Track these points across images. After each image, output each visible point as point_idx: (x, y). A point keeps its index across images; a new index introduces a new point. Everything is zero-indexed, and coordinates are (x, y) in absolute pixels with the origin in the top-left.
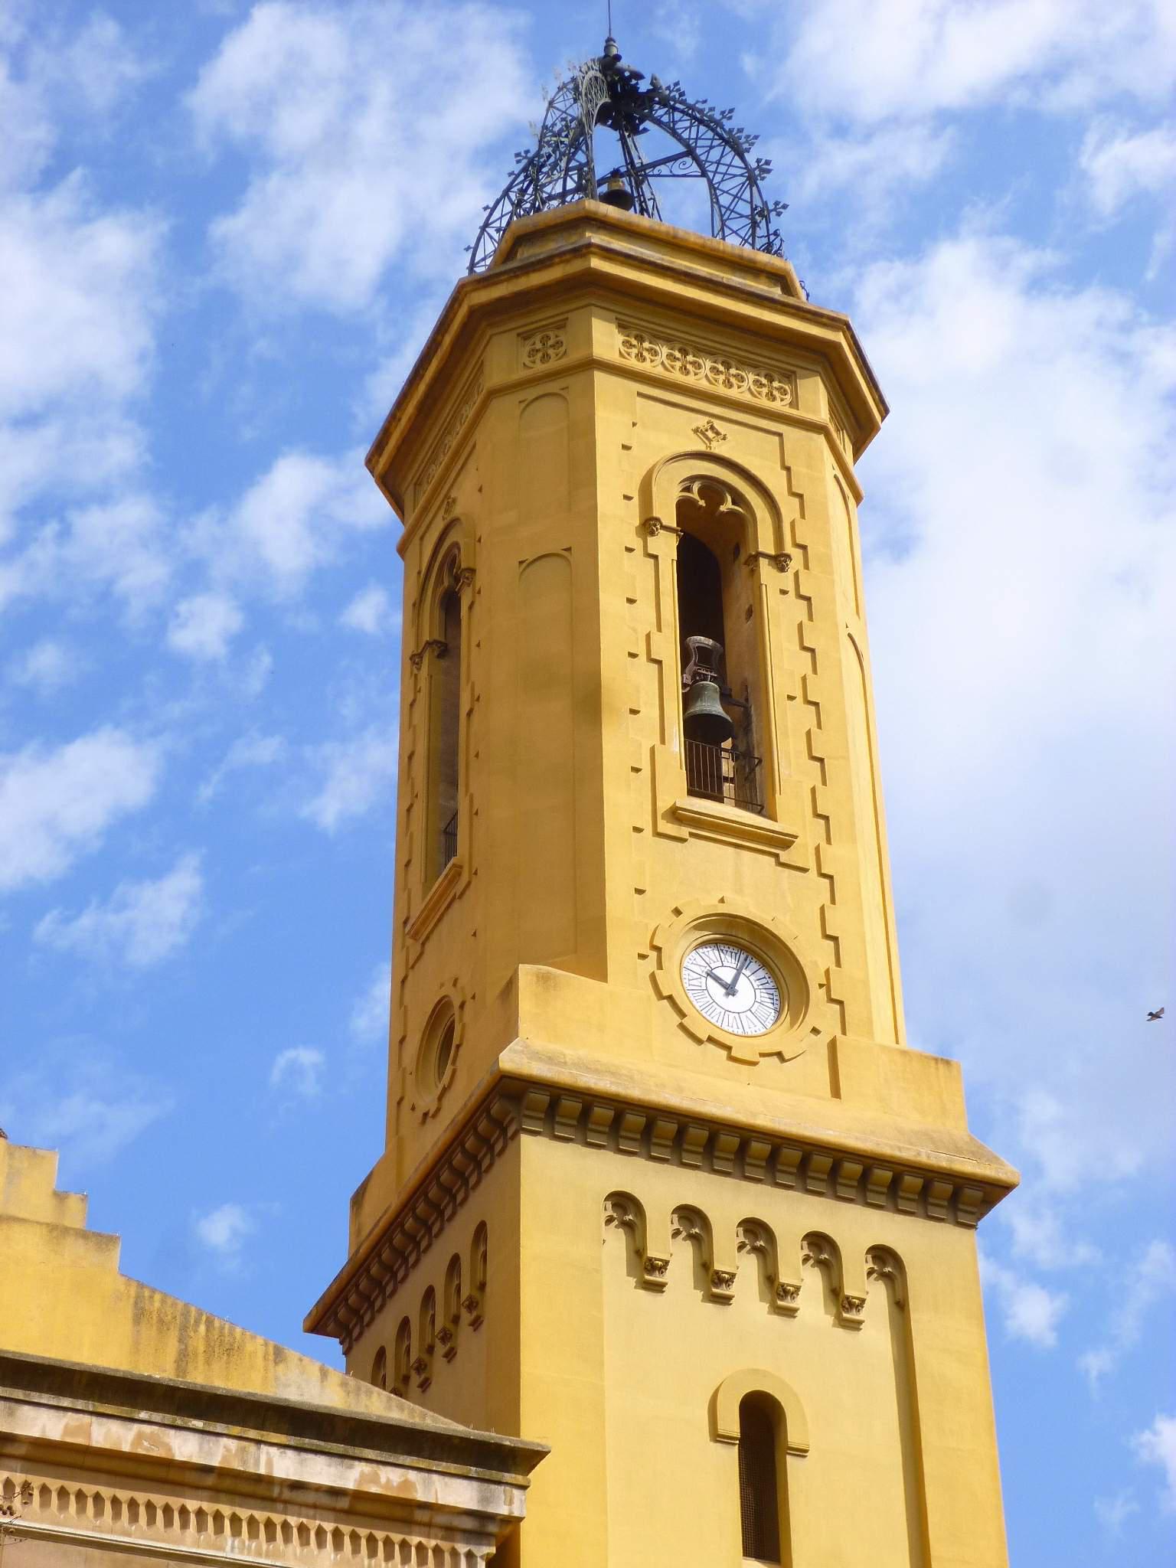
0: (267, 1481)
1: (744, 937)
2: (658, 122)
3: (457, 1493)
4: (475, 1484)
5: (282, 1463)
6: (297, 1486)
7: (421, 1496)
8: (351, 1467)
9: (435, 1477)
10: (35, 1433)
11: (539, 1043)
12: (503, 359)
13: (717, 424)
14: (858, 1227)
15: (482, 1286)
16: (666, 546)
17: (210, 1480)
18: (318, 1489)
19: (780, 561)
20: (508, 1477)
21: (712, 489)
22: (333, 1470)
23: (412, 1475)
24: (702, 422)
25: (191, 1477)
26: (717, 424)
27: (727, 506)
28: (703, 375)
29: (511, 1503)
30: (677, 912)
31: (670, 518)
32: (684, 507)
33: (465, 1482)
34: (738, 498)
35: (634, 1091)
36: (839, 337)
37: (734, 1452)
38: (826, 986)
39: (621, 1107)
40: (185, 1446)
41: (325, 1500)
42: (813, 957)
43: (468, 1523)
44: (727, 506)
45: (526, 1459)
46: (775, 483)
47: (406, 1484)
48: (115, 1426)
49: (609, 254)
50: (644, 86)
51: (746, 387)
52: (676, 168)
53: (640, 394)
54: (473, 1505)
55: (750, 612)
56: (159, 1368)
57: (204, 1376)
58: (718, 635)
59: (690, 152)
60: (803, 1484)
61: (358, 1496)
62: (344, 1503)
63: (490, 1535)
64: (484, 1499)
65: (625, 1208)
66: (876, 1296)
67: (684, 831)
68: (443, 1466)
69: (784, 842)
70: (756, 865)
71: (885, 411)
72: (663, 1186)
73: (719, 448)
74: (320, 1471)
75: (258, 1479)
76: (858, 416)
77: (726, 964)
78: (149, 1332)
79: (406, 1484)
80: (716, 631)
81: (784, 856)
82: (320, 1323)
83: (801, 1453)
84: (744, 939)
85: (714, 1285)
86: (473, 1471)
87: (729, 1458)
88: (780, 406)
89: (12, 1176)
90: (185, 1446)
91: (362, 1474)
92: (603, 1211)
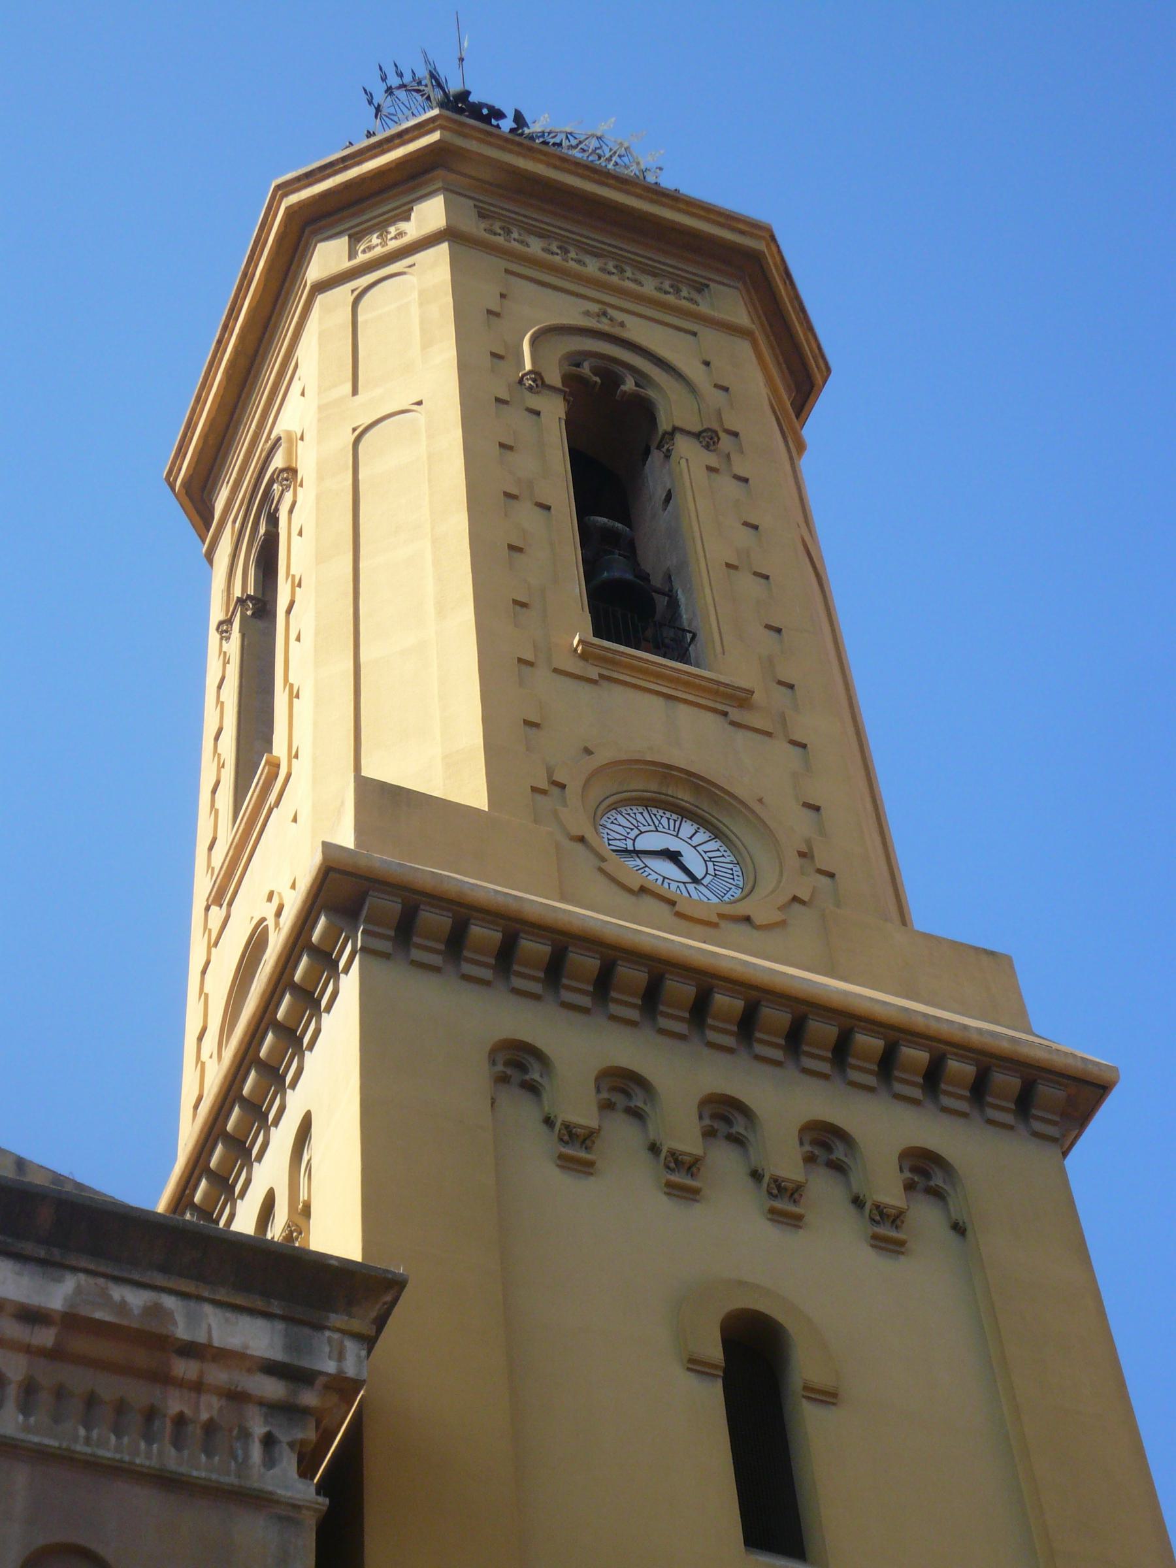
1: (684, 796)
4: (280, 1326)
7: (182, 1332)
8: (60, 1280)
9: (208, 1309)
13: (610, 311)
14: (884, 1128)
15: (307, 1211)
19: (708, 438)
22: (25, 1281)
23: (169, 1302)
26: (610, 311)
27: (629, 385)
29: (341, 1357)
30: (588, 751)
33: (260, 1323)
36: (760, 246)
37: (716, 1390)
44: (629, 385)
47: (155, 1311)
53: (507, 271)
54: (277, 1354)
55: (668, 497)
58: (627, 520)
60: (833, 1454)
62: (46, 1337)
63: (305, 1411)
64: (292, 1346)
65: (518, 1065)
67: (593, 672)
68: (222, 1295)
79: (155, 1311)
80: (624, 513)
81: (735, 714)
83: (827, 1397)
86: (276, 1307)
87: (710, 1397)
91: (78, 1290)
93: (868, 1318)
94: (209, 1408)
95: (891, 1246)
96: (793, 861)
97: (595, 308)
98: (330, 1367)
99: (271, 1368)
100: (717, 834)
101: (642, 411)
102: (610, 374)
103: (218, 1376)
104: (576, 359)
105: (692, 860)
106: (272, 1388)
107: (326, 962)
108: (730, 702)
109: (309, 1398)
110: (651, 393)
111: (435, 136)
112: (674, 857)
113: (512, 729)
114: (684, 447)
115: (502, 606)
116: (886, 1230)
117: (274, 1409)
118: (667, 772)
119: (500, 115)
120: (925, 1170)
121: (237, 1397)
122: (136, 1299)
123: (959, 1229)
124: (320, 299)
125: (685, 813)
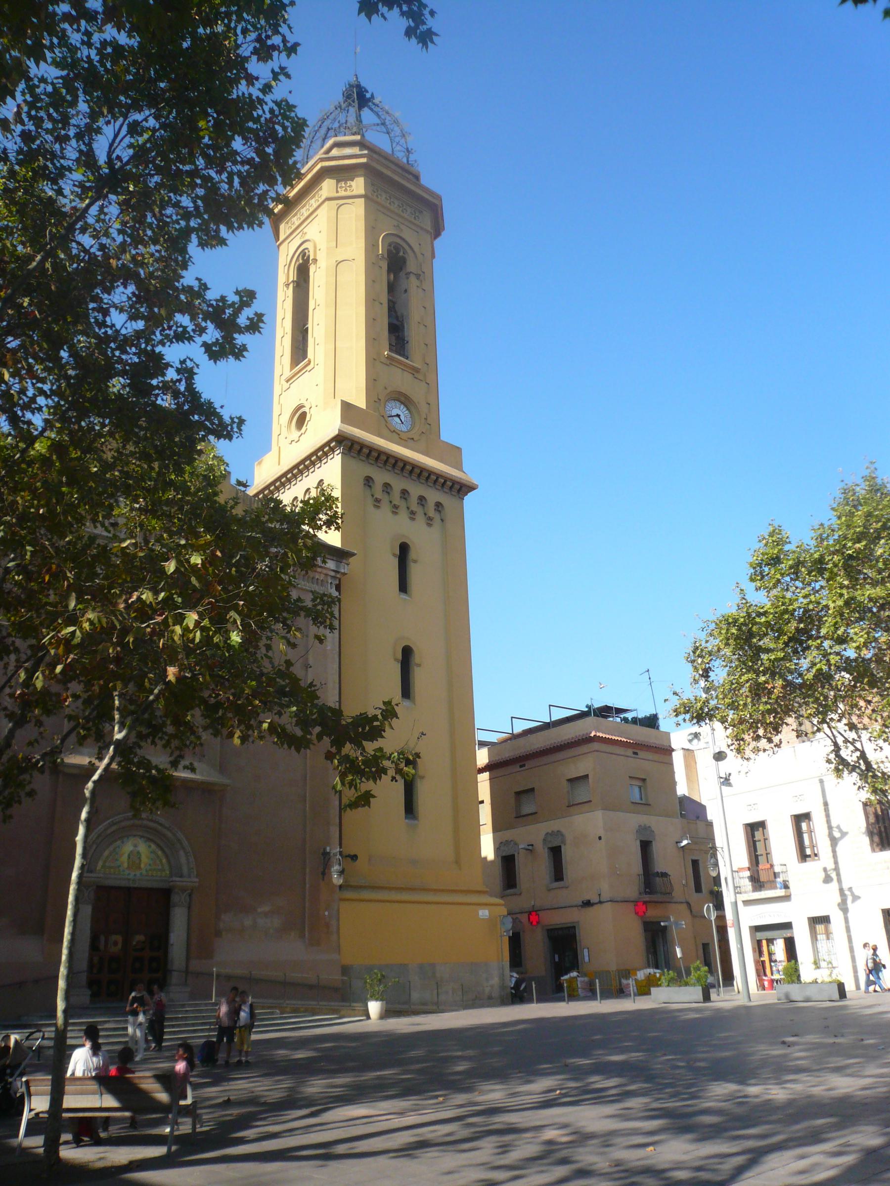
1: (403, 399)
2: (371, 109)
12: (328, 187)
14: (433, 496)
19: (418, 276)
32: (389, 252)
38: (426, 419)
42: (424, 408)
43: (333, 574)
44: (401, 254)
46: (416, 248)
50: (368, 95)
52: (378, 128)
54: (334, 568)
55: (406, 291)
59: (383, 124)
64: (337, 566)
66: (437, 518)
69: (417, 370)
70: (408, 377)
72: (381, 477)
76: (437, 230)
83: (415, 561)
84: (404, 399)
85: (395, 509)
92: (362, 481)
93: (424, 539)
94: (322, 577)
95: (429, 525)
96: (423, 421)
99: (333, 571)
100: (408, 409)
102: (397, 248)
103: (325, 571)
105: (402, 418)
106: (333, 574)
107: (332, 450)
108: (415, 371)
109: (338, 576)
110: (406, 256)
111: (364, 160)
112: (398, 416)
113: (372, 382)
114: (413, 278)
115: (371, 341)
116: (429, 521)
117: (333, 577)
118: (400, 393)
119: (367, 92)
120: (439, 506)
121: (326, 575)
123: (442, 520)
124: (327, 203)
125: (402, 403)
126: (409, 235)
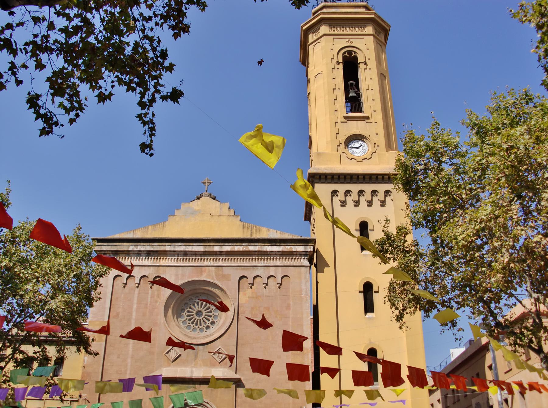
0: (267, 251)
3: (300, 248)
5: (268, 248)
6: (272, 251)
7: (294, 250)
10: (226, 250)
11: (317, 167)
16: (341, 66)
17: (257, 253)
18: (275, 251)
20: (310, 244)
21: (350, 52)
24: (348, 40)
25: (253, 253)
26: (351, 40)
28: (348, 31)
31: (341, 60)
32: (344, 58)
34: (355, 53)
35: (335, 172)
39: (333, 175)
40: (252, 248)
41: (277, 253)
43: (304, 253)
44: (353, 54)
45: (313, 241)
47: (291, 248)
48: (239, 247)
49: (324, 13)
51: (357, 31)
56: (247, 236)
57: (255, 236)
61: (283, 251)
62: (281, 253)
64: (305, 249)
67: (346, 121)
70: (361, 124)
71: (390, 27)
73: (352, 45)
74: (275, 248)
75: (265, 251)
77: (356, 144)
78: (246, 230)
81: (367, 120)
82: (305, 220)
88: (363, 33)
89: (221, 209)
90: (252, 248)
97: (348, 40)
98: (309, 250)
100: (364, 142)
101: (356, 58)
104: (344, 53)
106: (304, 253)
110: (357, 55)
122: (289, 247)
126: (356, 42)
